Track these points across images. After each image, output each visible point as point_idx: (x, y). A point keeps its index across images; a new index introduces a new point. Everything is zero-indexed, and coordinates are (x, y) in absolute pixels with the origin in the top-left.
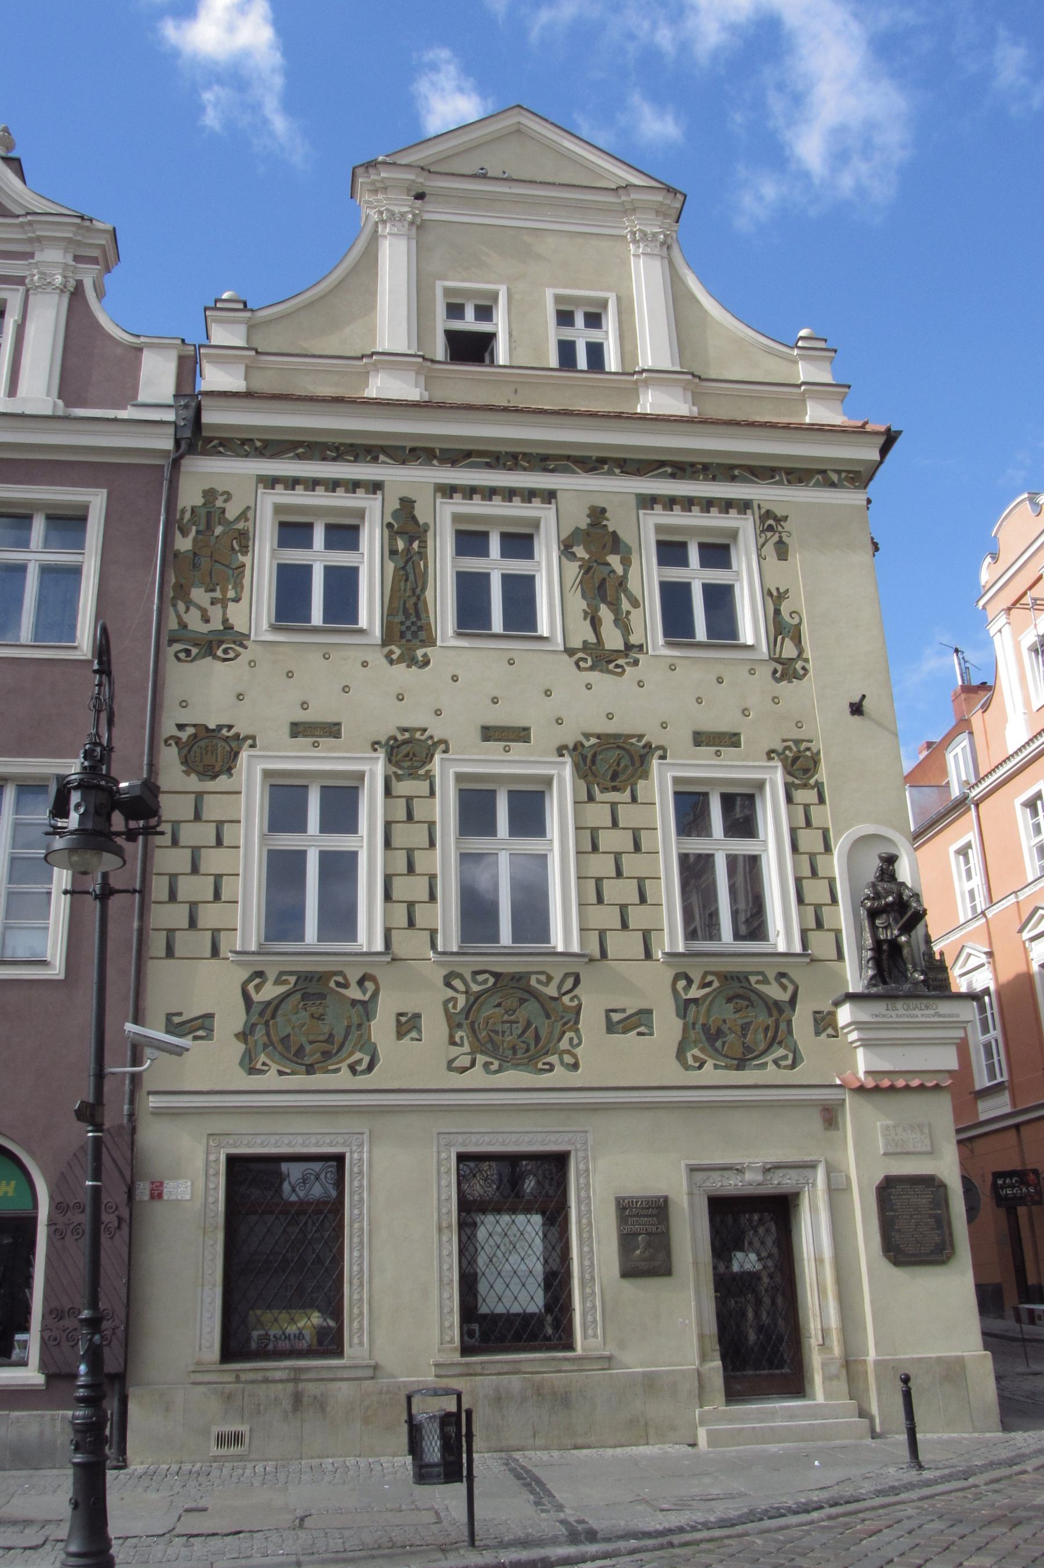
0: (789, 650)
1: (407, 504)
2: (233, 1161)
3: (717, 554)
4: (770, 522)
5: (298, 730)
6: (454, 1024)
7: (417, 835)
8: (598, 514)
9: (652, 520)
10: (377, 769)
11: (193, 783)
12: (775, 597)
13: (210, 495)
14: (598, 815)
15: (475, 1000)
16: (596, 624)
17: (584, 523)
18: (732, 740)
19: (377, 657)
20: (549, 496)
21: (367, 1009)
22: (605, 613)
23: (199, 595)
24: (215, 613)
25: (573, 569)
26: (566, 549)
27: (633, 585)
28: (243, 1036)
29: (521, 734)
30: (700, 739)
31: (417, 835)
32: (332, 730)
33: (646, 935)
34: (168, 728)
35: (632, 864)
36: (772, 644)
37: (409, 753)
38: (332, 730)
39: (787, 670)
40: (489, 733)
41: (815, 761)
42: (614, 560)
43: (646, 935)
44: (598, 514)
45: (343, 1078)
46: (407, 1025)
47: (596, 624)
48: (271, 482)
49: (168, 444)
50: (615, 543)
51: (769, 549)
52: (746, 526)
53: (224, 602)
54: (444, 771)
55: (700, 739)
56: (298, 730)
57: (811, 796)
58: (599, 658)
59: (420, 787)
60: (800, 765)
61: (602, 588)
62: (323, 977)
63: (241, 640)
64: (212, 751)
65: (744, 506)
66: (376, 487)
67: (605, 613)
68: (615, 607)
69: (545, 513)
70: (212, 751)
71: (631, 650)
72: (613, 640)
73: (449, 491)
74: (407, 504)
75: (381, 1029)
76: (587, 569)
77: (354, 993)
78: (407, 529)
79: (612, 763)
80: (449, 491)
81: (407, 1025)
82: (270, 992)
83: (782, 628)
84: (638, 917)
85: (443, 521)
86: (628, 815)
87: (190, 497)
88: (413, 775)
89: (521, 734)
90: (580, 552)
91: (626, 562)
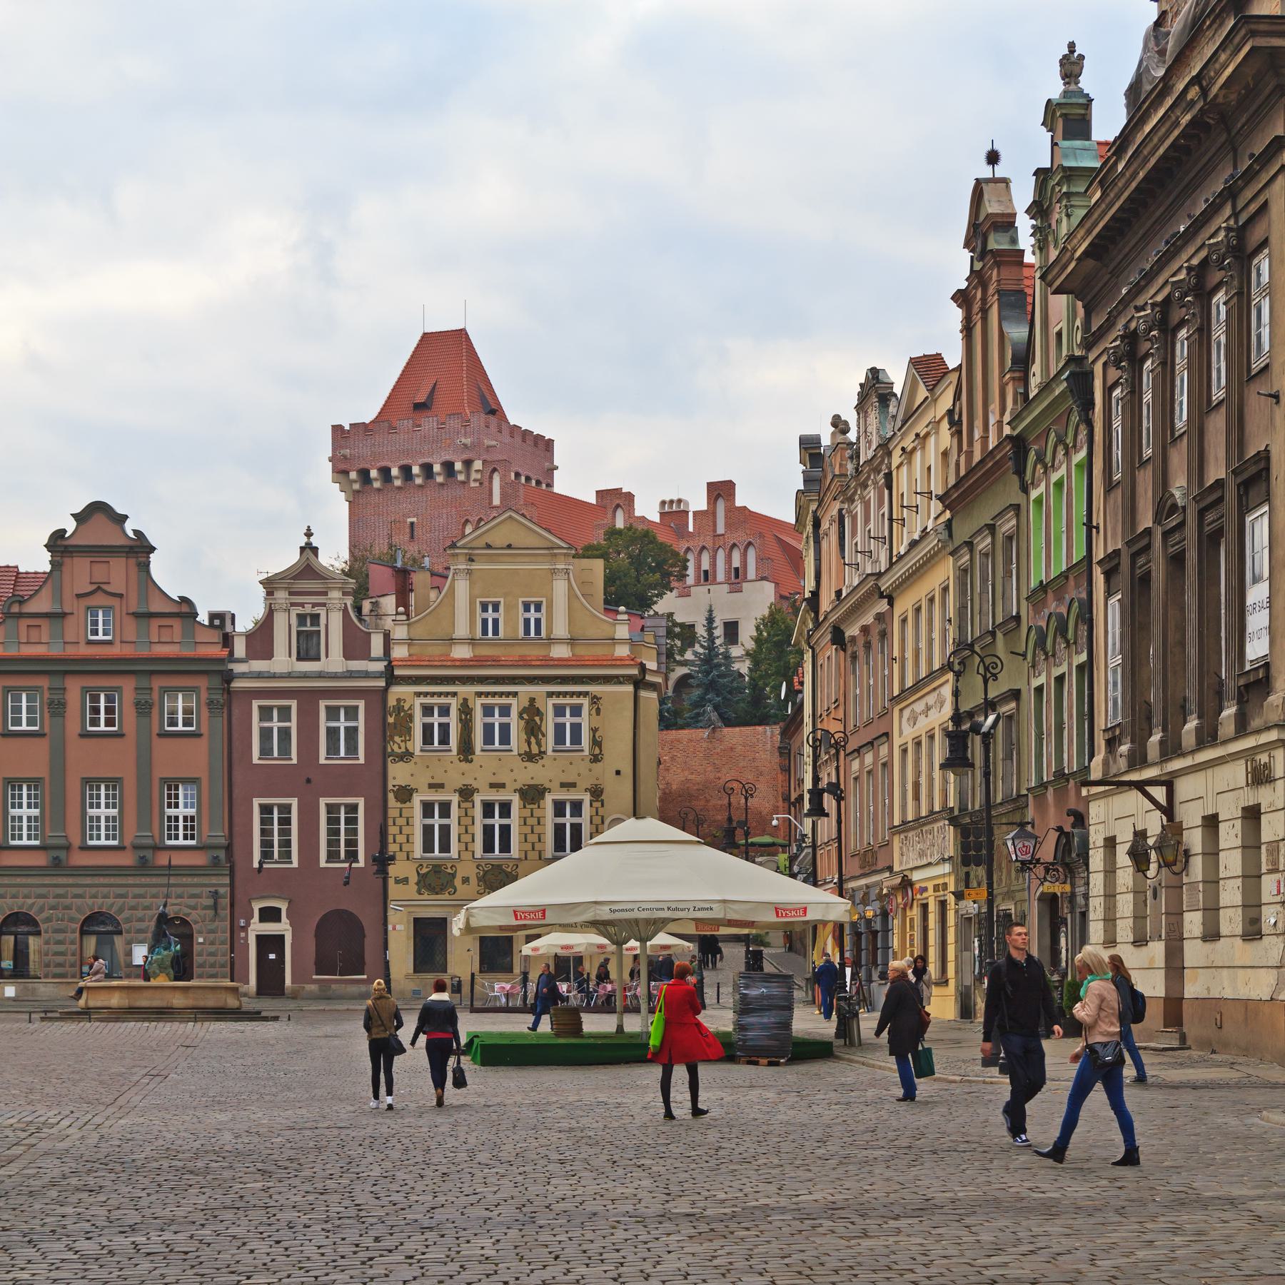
0: (597, 751)
1: (465, 700)
2: (415, 919)
3: (576, 711)
4: (595, 700)
5: (431, 786)
6: (479, 880)
7: (469, 821)
8: (532, 700)
9: (552, 701)
10: (455, 799)
11: (399, 805)
12: (594, 731)
13: (399, 700)
14: (527, 813)
15: (486, 873)
16: (529, 744)
17: (527, 704)
18: (573, 785)
19: (456, 760)
20: (515, 694)
21: (454, 875)
22: (533, 740)
23: (397, 739)
24: (403, 745)
25: (522, 723)
26: (520, 717)
27: (543, 729)
28: (417, 884)
29: (503, 786)
30: (563, 785)
31: (469, 821)
32: (441, 786)
33: (540, 852)
34: (390, 787)
35: (537, 829)
36: (591, 749)
37: (466, 793)
38: (441, 786)
39: (596, 759)
40: (492, 786)
41: (602, 792)
42: (537, 719)
43: (540, 852)
44: (532, 700)
45: (446, 896)
46: (466, 880)
47: (529, 744)
48: (418, 694)
49: (383, 684)
50: (538, 712)
51: (594, 711)
52: (585, 702)
53: (405, 741)
54: (478, 799)
55: (563, 785)
56: (431, 786)
57: (599, 804)
58: (529, 757)
59: (470, 805)
60: (596, 793)
61: (533, 730)
62: (440, 866)
63: (412, 755)
64: (405, 794)
65: (586, 694)
66: (454, 694)
67: (533, 740)
68: (536, 737)
69: (512, 701)
70: (405, 794)
71: (542, 753)
72: (535, 750)
73: (479, 694)
74: (465, 700)
75: (458, 882)
76: (527, 722)
77: (449, 871)
78: (466, 710)
79: (532, 794)
80: (479, 694)
81: (466, 880)
82: (424, 870)
83: (596, 743)
84: (538, 846)
85: (477, 705)
86: (537, 813)
87: (392, 702)
88: (466, 801)
89: (503, 786)
90: (525, 716)
91: (541, 720)
